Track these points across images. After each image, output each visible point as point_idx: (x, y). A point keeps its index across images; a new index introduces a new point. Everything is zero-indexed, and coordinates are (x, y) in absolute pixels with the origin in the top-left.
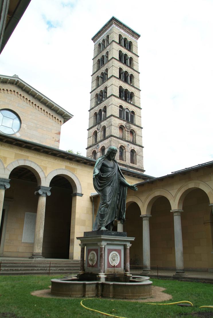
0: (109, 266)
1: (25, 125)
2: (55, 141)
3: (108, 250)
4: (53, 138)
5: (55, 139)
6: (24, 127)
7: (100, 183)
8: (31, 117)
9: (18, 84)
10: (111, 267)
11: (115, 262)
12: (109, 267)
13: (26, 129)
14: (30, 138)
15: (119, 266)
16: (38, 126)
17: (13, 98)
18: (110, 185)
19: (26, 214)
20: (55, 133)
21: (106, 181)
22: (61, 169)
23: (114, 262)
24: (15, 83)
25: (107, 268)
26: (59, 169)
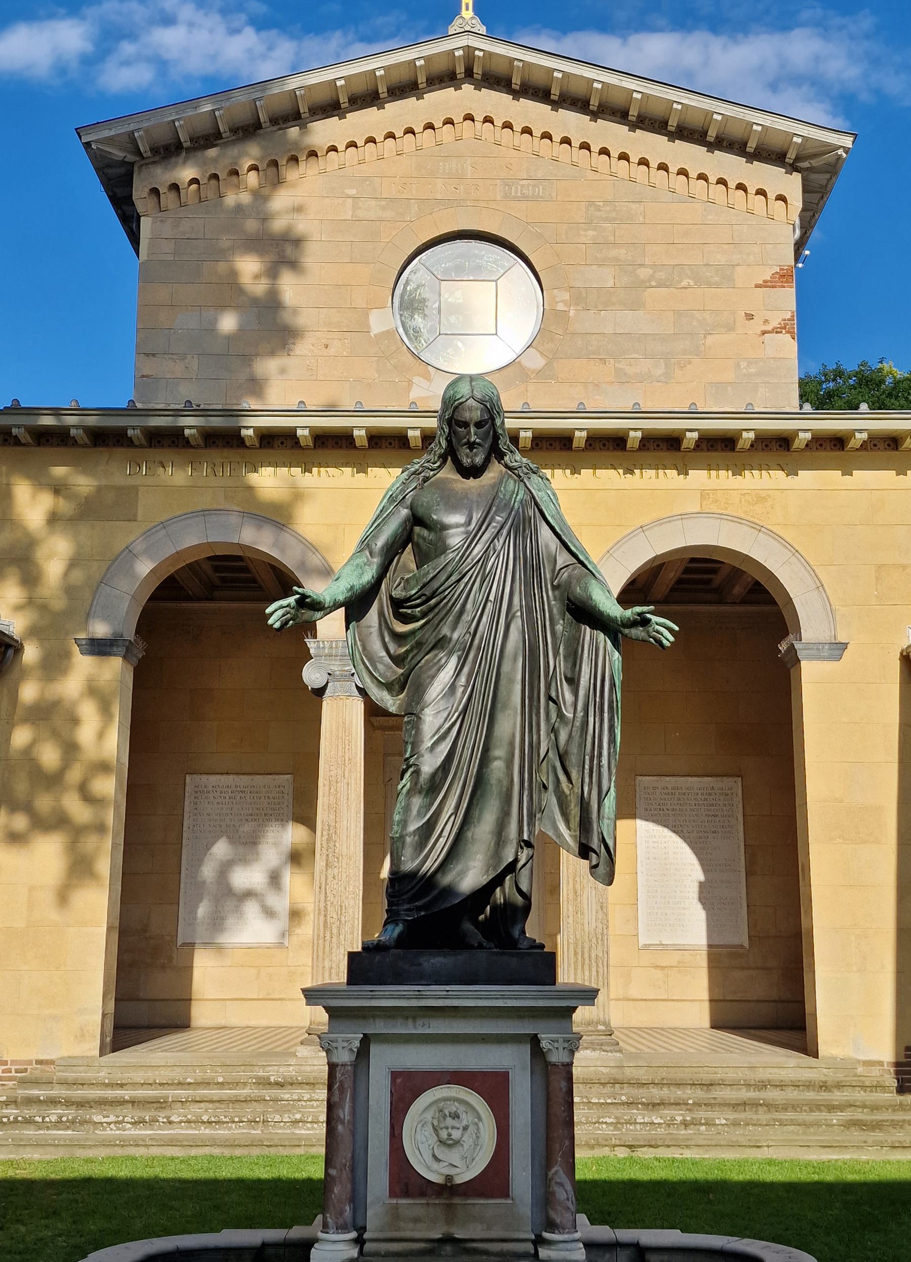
0: (406, 1183)
1: (566, 296)
2: (764, 333)
3: (395, 1075)
4: (750, 317)
5: (766, 321)
6: (561, 307)
7: (399, 638)
8: (591, 233)
9: (477, 70)
10: (423, 1194)
11: (464, 1158)
12: (406, 1193)
13: (572, 313)
14: (603, 361)
15: (493, 1182)
16: (644, 273)
17: (469, 162)
18: (441, 643)
19: (728, 782)
20: (758, 286)
21: (423, 621)
22: (671, 519)
23: (454, 1156)
24: (460, 70)
25: (393, 1194)
26: (660, 522)
